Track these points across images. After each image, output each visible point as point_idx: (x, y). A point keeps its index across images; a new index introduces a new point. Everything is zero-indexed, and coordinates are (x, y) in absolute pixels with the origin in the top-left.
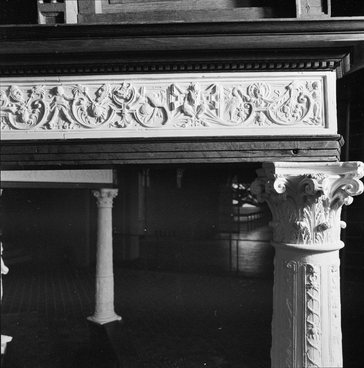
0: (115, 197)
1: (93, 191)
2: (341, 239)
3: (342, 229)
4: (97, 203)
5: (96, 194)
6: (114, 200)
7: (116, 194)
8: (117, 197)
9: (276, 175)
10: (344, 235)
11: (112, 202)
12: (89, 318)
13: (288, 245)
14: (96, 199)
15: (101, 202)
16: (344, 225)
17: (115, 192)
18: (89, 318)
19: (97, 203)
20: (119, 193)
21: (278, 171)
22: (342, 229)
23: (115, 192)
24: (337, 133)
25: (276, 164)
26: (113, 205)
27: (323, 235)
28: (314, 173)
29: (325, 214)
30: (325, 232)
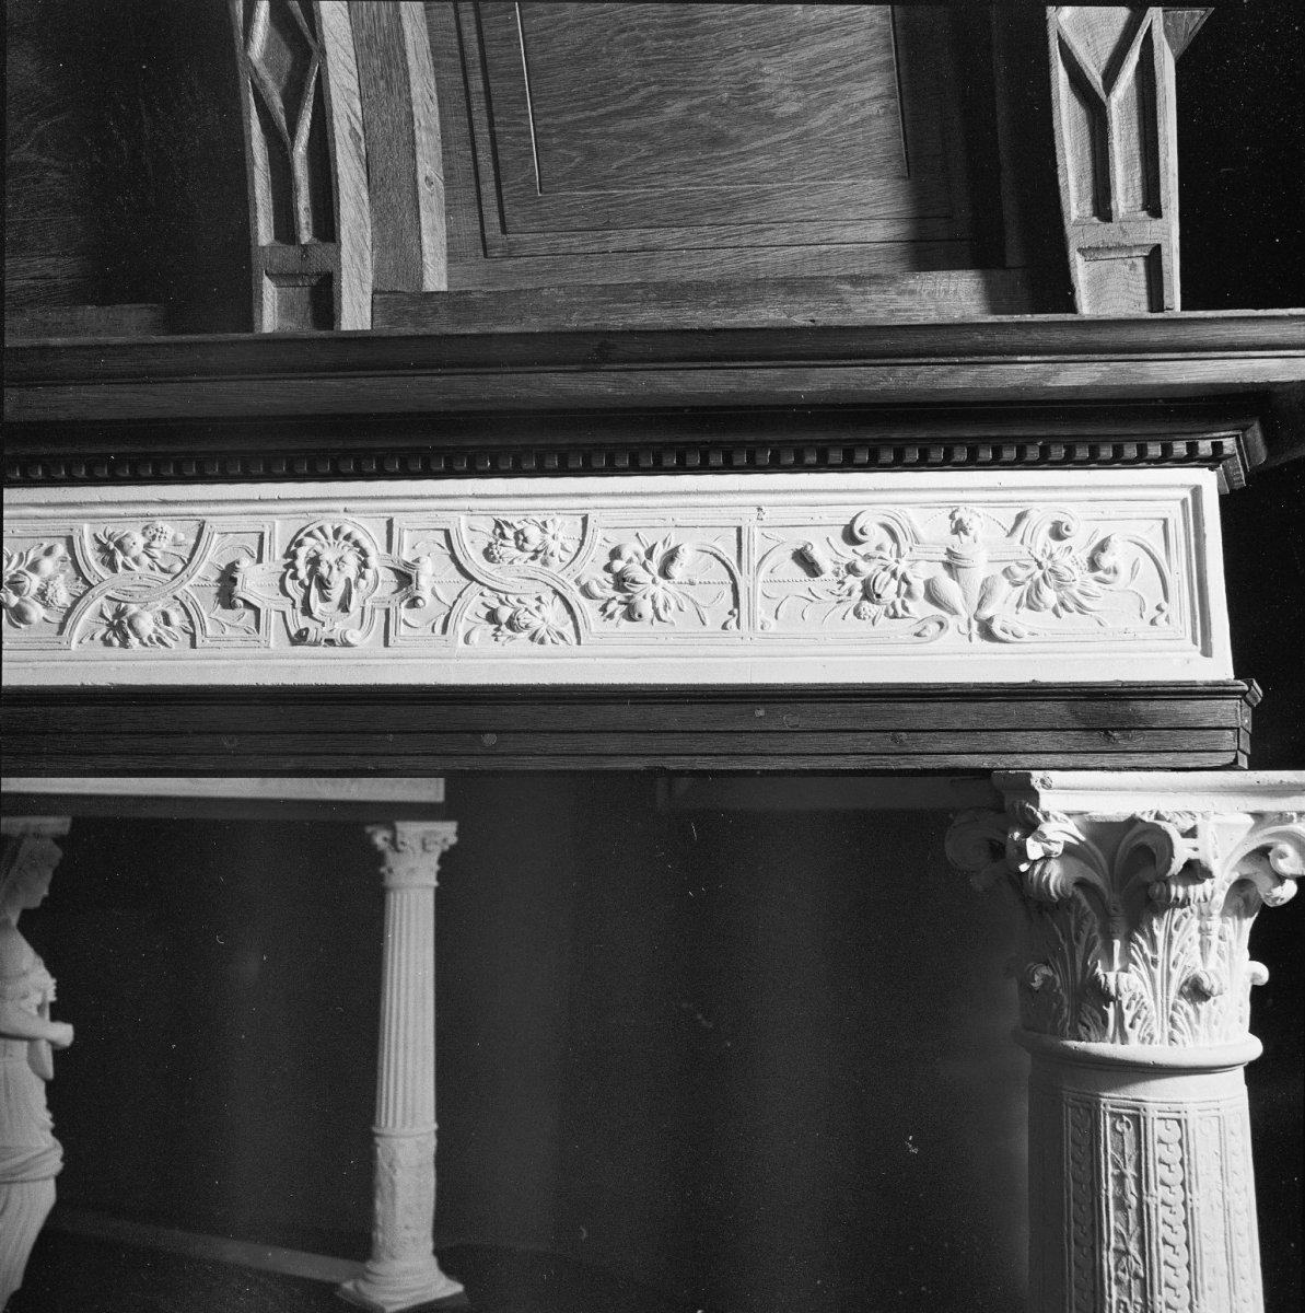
0: (447, 848)
1: (369, 829)
2: (1253, 1030)
4: (383, 870)
5: (380, 839)
6: (444, 859)
7: (453, 840)
8: (453, 848)
10: (1266, 1010)
13: (1073, 1044)
14: (379, 858)
16: (1262, 973)
17: (447, 832)
19: (383, 870)
20: (458, 834)
21: (1048, 801)
22: (1255, 988)
23: (447, 832)
24: (1231, 675)
26: (440, 876)
27: (1197, 1012)
28: (1165, 805)
29: (1201, 943)
30: (1203, 1007)
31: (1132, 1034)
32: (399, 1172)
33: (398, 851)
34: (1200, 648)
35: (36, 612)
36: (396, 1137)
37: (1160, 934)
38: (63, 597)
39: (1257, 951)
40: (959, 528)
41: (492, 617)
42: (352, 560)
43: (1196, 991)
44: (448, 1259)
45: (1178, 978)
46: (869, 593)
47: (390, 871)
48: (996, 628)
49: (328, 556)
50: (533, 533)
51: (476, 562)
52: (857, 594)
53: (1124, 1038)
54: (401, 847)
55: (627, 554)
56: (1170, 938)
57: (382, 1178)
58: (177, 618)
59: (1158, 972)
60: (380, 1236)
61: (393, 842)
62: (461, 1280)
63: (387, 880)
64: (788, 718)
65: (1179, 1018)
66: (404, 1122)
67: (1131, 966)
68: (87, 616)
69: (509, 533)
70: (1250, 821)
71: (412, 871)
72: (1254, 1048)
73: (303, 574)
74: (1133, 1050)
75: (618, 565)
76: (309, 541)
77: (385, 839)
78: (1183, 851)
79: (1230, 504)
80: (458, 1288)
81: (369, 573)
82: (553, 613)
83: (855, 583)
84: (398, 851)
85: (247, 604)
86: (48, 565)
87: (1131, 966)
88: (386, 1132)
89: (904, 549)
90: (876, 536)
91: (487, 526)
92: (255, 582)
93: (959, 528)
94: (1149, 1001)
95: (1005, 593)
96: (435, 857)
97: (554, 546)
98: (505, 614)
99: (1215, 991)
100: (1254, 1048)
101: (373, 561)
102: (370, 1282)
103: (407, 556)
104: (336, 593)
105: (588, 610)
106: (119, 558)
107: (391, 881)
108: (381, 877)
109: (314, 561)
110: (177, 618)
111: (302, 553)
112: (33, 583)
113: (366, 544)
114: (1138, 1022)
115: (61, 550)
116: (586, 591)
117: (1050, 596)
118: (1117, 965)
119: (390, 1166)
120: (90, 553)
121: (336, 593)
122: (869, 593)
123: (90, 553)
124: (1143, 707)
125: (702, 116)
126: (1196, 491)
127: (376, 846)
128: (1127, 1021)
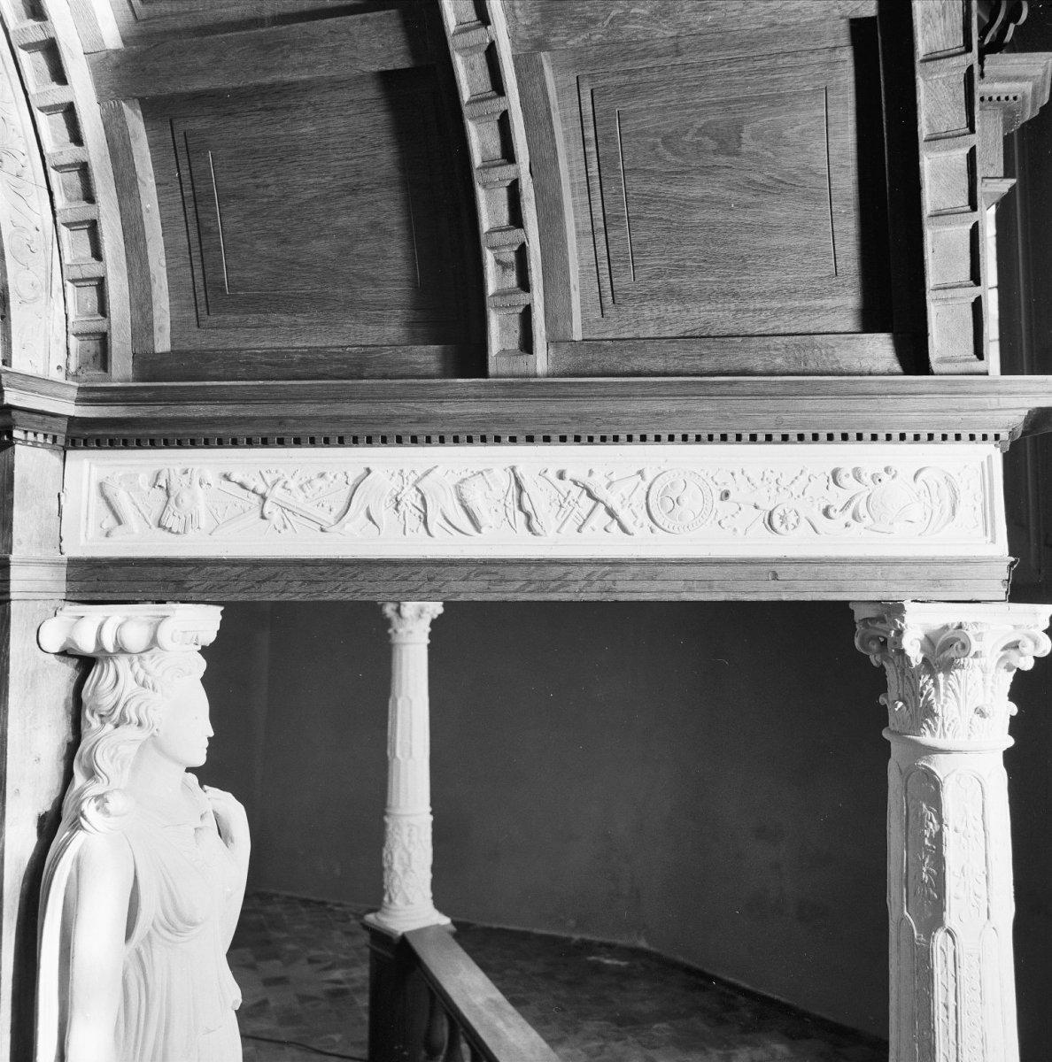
0: (435, 616)
2: (1011, 732)
3: (1012, 717)
4: (390, 631)
5: (389, 610)
6: (434, 623)
8: (439, 615)
9: (906, 626)
11: (429, 629)
12: (370, 917)
14: (388, 623)
15: (400, 631)
18: (370, 917)
19: (390, 631)
25: (908, 605)
26: (431, 636)
31: (949, 734)
34: (989, 538)
39: (1014, 696)
43: (981, 712)
44: (440, 903)
47: (395, 631)
61: (398, 611)
62: (446, 914)
63: (393, 638)
67: (948, 700)
70: (1011, 628)
71: (410, 632)
72: (1010, 742)
77: (393, 610)
78: (975, 646)
79: (1009, 460)
80: (445, 921)
87: (948, 700)
96: (428, 622)
99: (991, 715)
100: (1010, 742)
107: (396, 639)
108: (389, 636)
114: (951, 728)
118: (942, 698)
126: (989, 457)
127: (385, 614)
128: (946, 729)
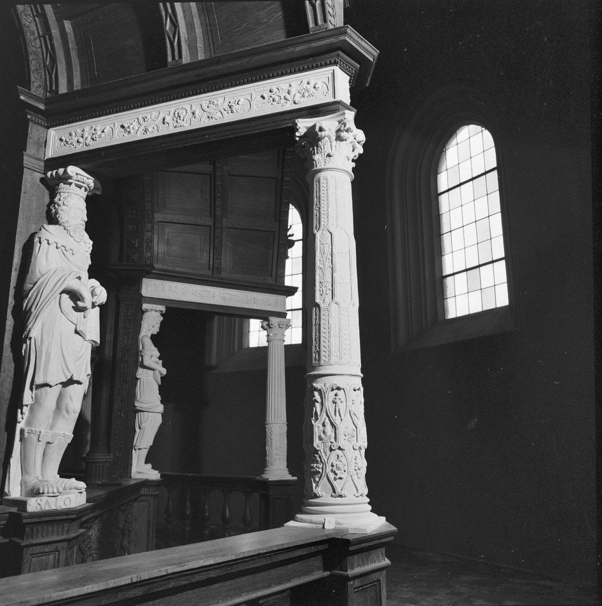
21: (299, 125)
30: (331, 158)
31: (318, 166)
32: (273, 435)
33: (271, 328)
35: (132, 131)
36: (272, 424)
37: (322, 147)
38: (137, 128)
40: (290, 86)
41: (208, 117)
42: (185, 112)
45: (326, 154)
46: (274, 100)
48: (296, 102)
49: (180, 112)
50: (216, 102)
51: (205, 108)
52: (272, 101)
53: (317, 166)
54: (271, 326)
55: (231, 102)
56: (324, 147)
57: (268, 439)
58: (155, 128)
59: (323, 154)
60: (268, 458)
64: (258, 123)
65: (327, 162)
66: (275, 419)
68: (141, 130)
69: (211, 102)
73: (176, 116)
74: (318, 167)
75: (230, 104)
76: (178, 111)
77: (267, 325)
81: (188, 114)
82: (219, 114)
83: (271, 99)
84: (271, 328)
85: (167, 123)
86: (134, 123)
88: (269, 423)
89: (280, 91)
90: (275, 90)
91: (208, 102)
92: (168, 119)
93: (290, 86)
94: (321, 159)
95: (298, 95)
97: (219, 103)
98: (210, 116)
101: (188, 111)
102: (265, 473)
103: (194, 110)
104: (182, 119)
105: (225, 113)
106: (146, 120)
109: (178, 113)
110: (155, 128)
111: (176, 113)
112: (132, 126)
113: (187, 109)
115: (136, 120)
116: (224, 110)
117: (306, 94)
119: (270, 434)
120: (141, 120)
121: (182, 119)
122: (274, 100)
123: (141, 120)
124: (321, 109)
125: (249, 26)
